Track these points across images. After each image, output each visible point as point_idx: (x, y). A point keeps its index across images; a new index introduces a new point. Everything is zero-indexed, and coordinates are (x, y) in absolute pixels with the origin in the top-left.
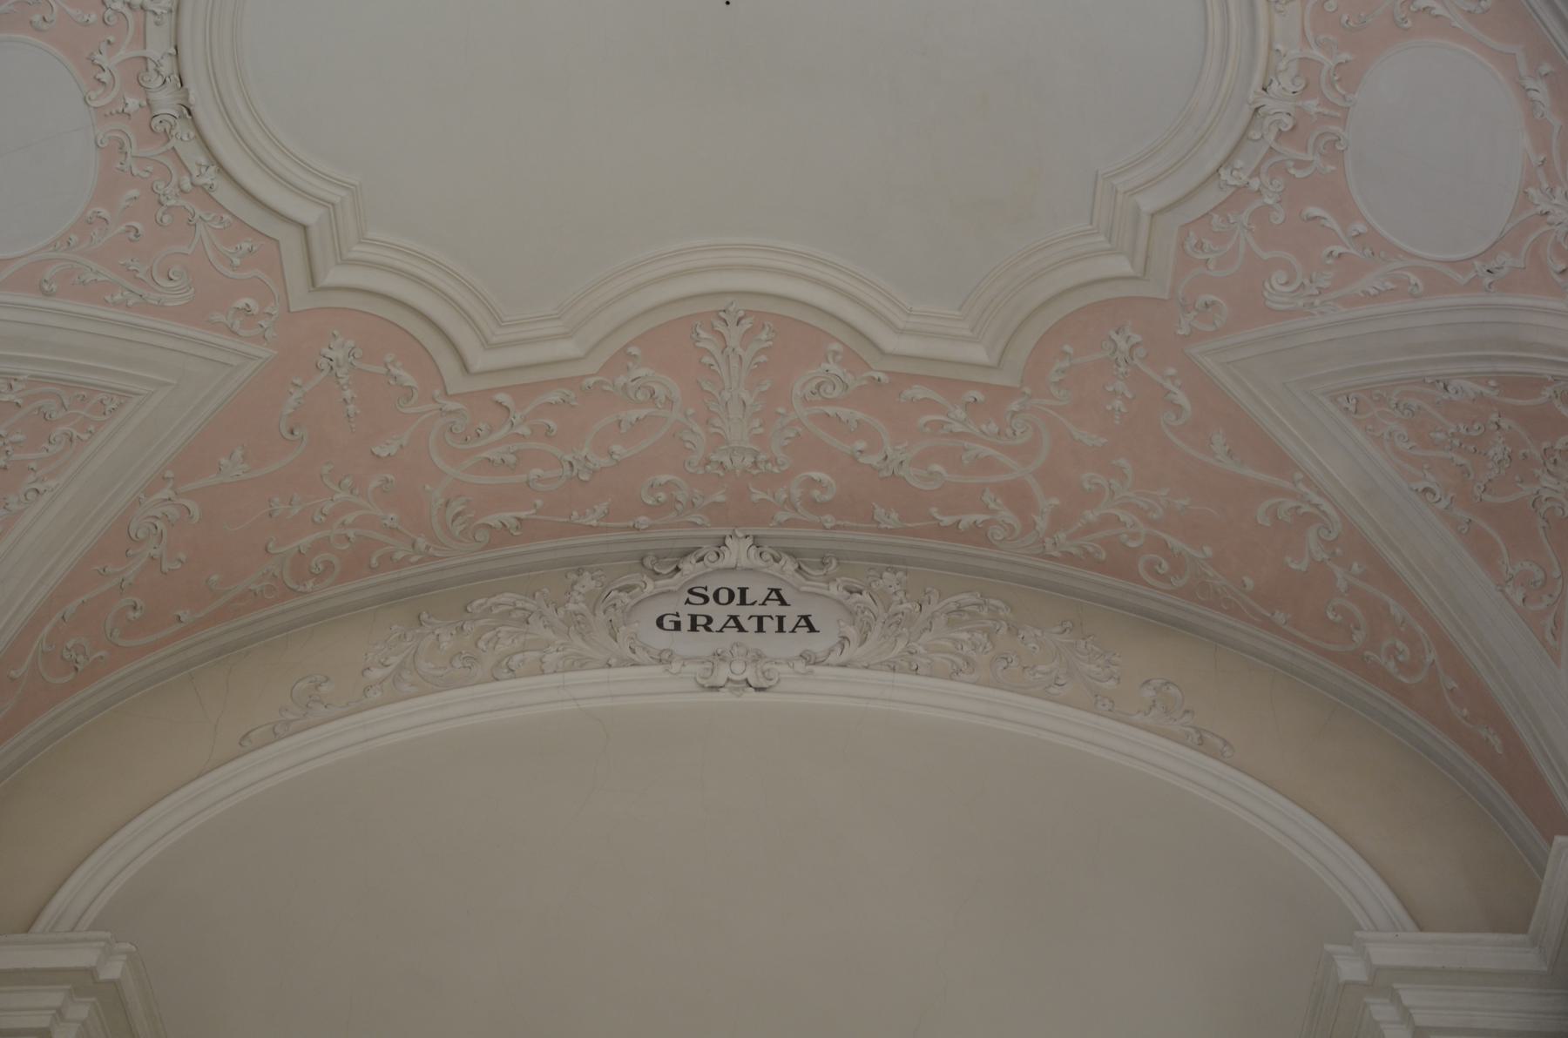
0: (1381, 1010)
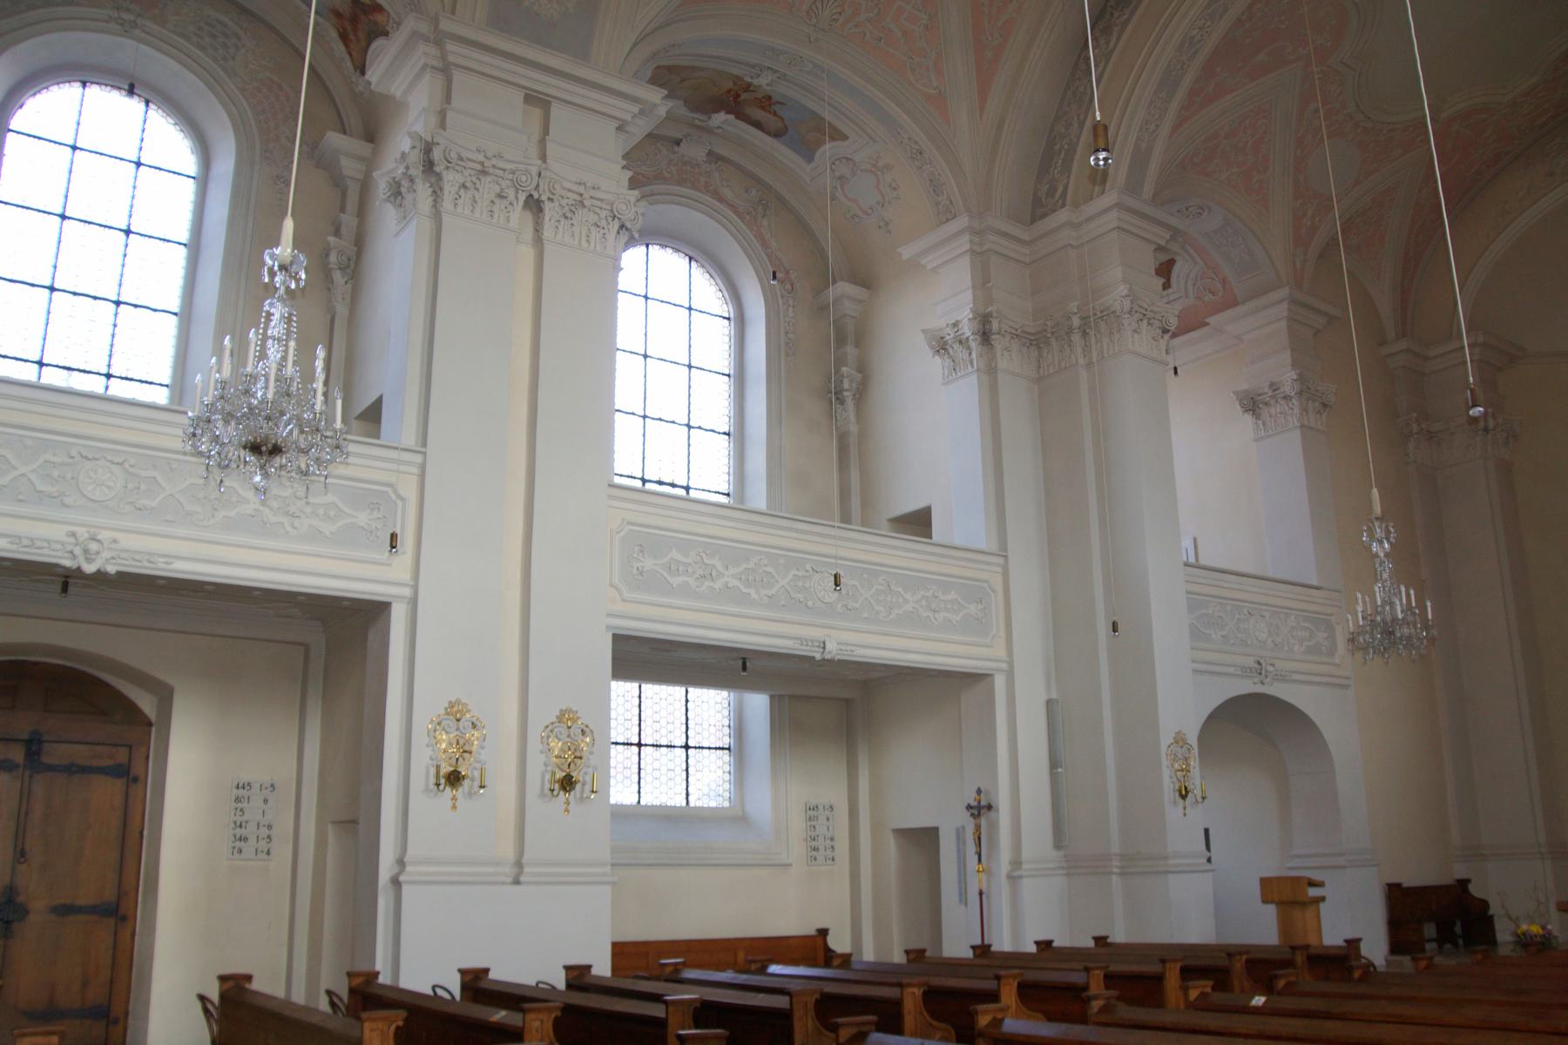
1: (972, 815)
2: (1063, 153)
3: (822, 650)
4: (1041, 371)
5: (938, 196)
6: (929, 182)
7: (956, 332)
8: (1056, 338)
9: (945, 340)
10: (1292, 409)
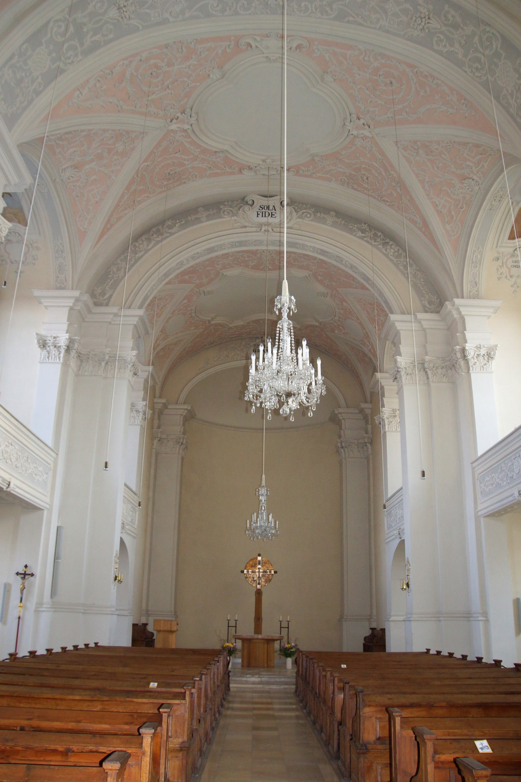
0: (339, 415)
1: (22, 578)
2: (113, 280)
3: (7, 486)
4: (80, 372)
5: (59, 273)
6: (58, 266)
7: (54, 341)
8: (92, 360)
9: (46, 342)
10: (138, 417)
